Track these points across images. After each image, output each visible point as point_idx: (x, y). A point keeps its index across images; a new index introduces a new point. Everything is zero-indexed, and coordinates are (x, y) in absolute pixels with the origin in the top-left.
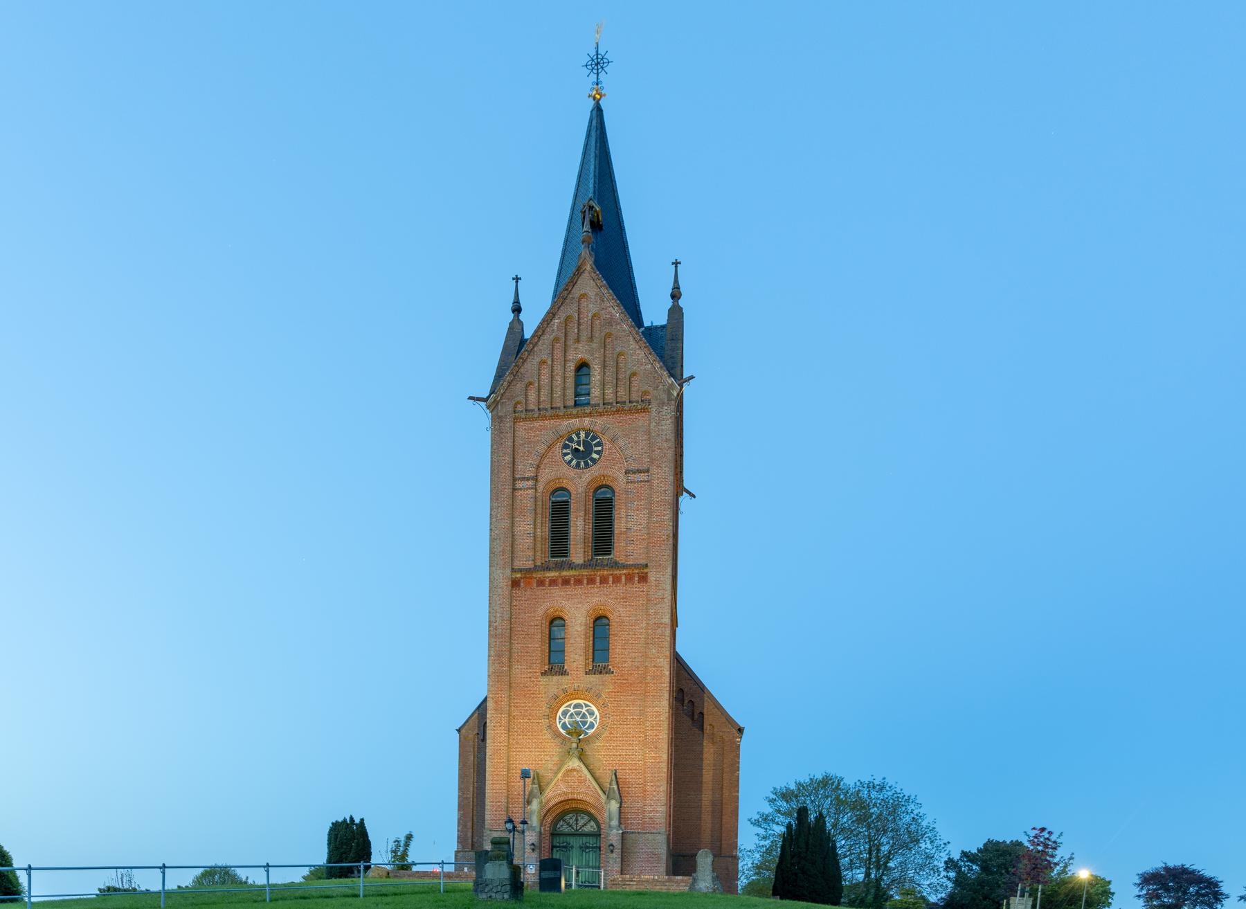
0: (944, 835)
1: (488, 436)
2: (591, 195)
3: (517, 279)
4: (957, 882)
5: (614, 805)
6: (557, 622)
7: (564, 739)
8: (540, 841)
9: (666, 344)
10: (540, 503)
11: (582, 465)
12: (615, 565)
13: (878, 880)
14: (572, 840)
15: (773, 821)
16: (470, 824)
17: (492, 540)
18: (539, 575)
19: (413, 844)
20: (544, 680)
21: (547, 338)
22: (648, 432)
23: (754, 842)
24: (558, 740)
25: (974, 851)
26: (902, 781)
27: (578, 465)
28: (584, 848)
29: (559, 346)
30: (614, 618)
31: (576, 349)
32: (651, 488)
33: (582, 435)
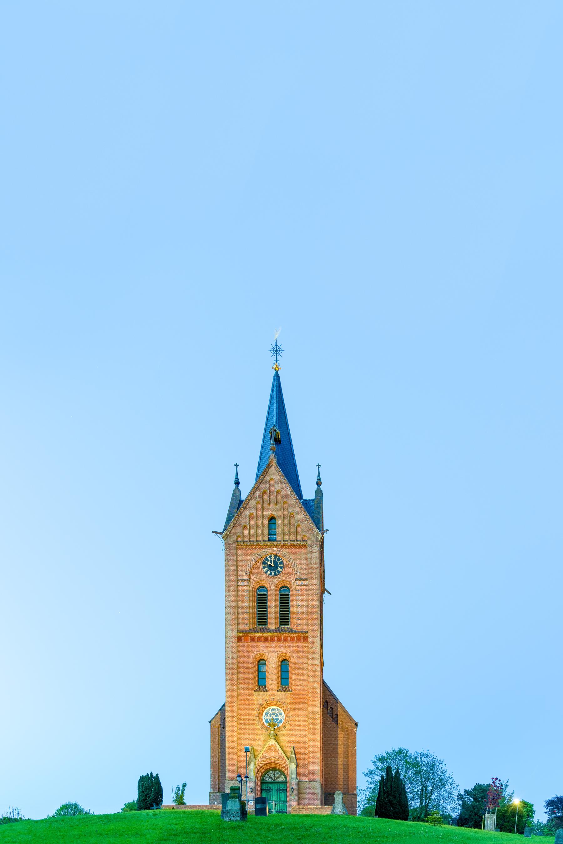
0: (457, 781)
1: (223, 554)
2: (274, 424)
3: (237, 465)
4: (463, 806)
5: (293, 766)
6: (262, 662)
7: (267, 728)
8: (255, 787)
9: (314, 509)
10: (251, 594)
11: (273, 574)
12: (291, 631)
13: (427, 806)
14: (273, 787)
15: (375, 773)
16: (217, 777)
17: (226, 614)
18: (252, 635)
19: (187, 789)
20: (255, 694)
21: (253, 502)
22: (306, 558)
23: (365, 785)
24: (264, 729)
25: (470, 790)
26: (438, 752)
27: (271, 574)
28: (278, 790)
29: (260, 507)
30: (291, 661)
31: (269, 509)
32: (308, 589)
33: (273, 557)
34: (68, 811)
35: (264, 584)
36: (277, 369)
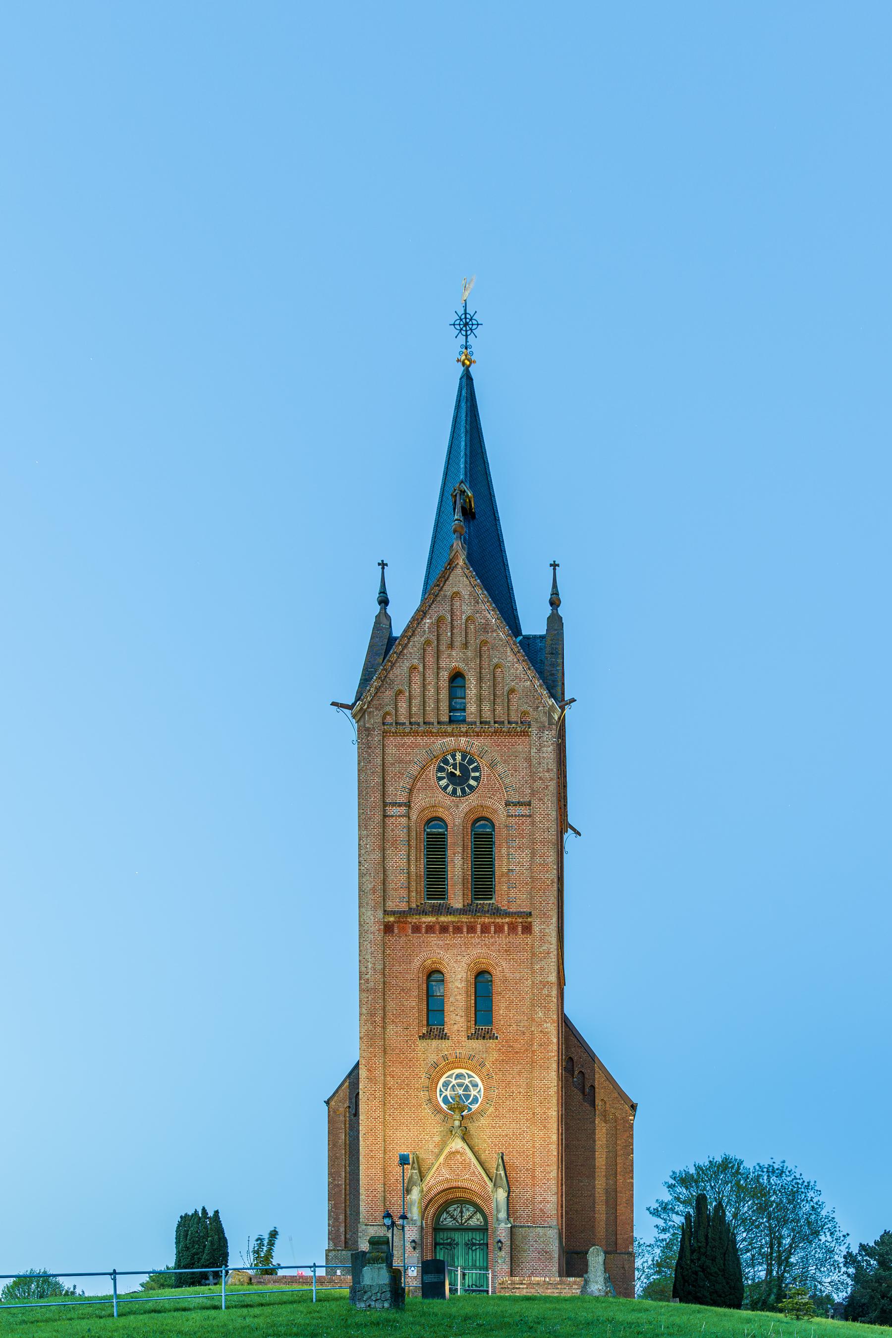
0: (843, 1227)
1: (353, 752)
3: (383, 565)
4: (856, 1278)
5: (501, 1194)
6: (436, 976)
7: (446, 1115)
8: (422, 1238)
9: (544, 657)
10: (413, 834)
11: (459, 792)
12: (497, 912)
13: (781, 1278)
14: (457, 1237)
15: (672, 1210)
16: (342, 1217)
17: (361, 875)
18: (414, 919)
19: (278, 1242)
20: (422, 1045)
21: (418, 640)
22: (529, 760)
23: (651, 1235)
25: (872, 1244)
27: (454, 792)
28: (470, 1245)
30: (497, 973)
31: (450, 656)
32: (533, 823)
33: (459, 757)
34: (29, 1289)
35: (441, 812)
36: (467, 363)
